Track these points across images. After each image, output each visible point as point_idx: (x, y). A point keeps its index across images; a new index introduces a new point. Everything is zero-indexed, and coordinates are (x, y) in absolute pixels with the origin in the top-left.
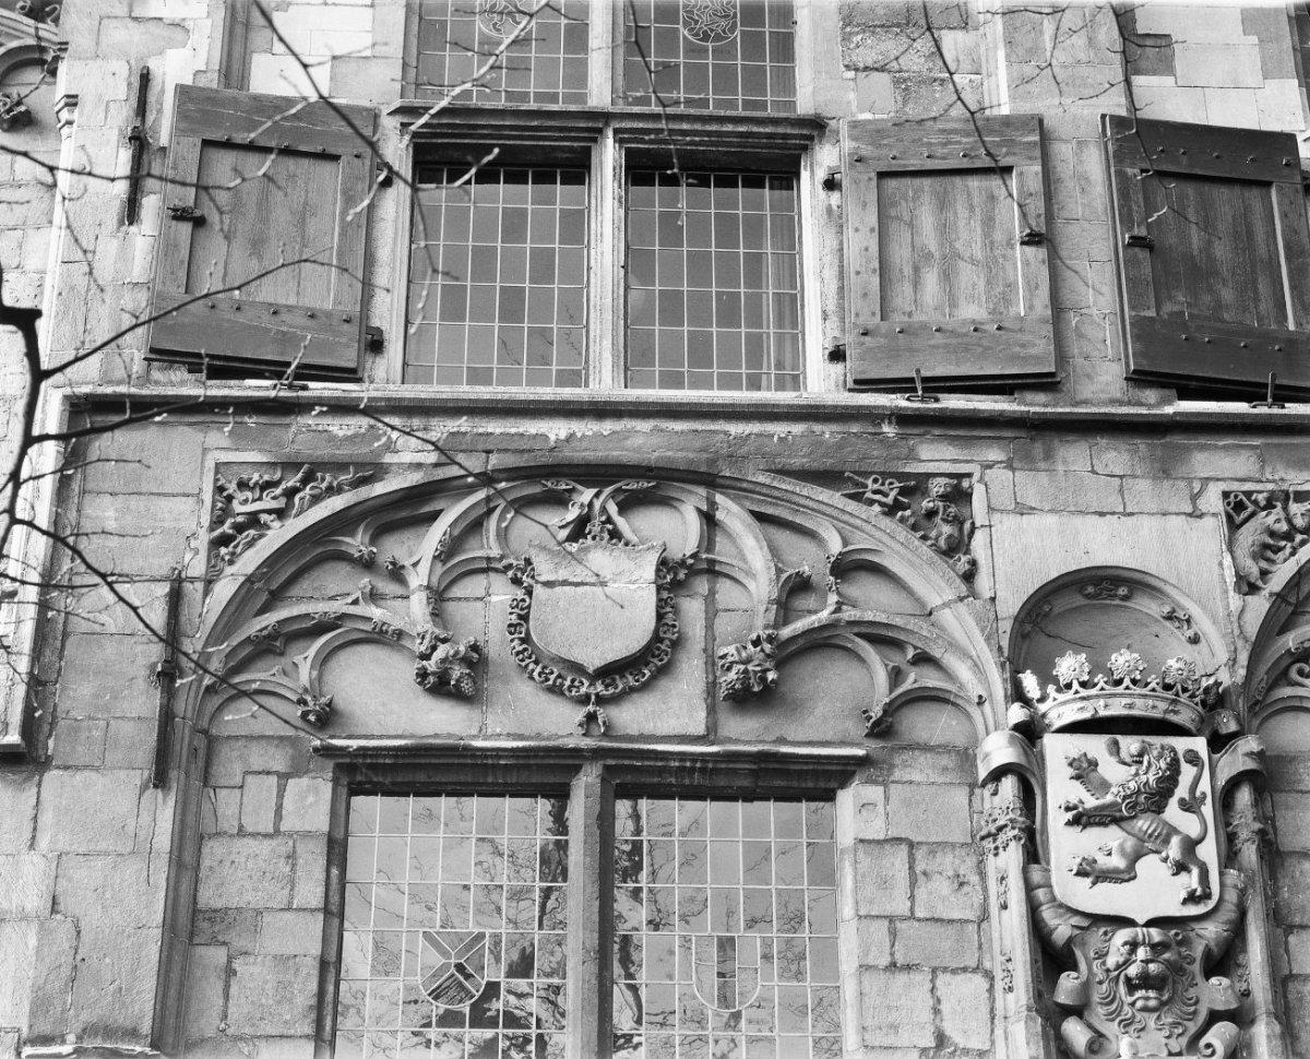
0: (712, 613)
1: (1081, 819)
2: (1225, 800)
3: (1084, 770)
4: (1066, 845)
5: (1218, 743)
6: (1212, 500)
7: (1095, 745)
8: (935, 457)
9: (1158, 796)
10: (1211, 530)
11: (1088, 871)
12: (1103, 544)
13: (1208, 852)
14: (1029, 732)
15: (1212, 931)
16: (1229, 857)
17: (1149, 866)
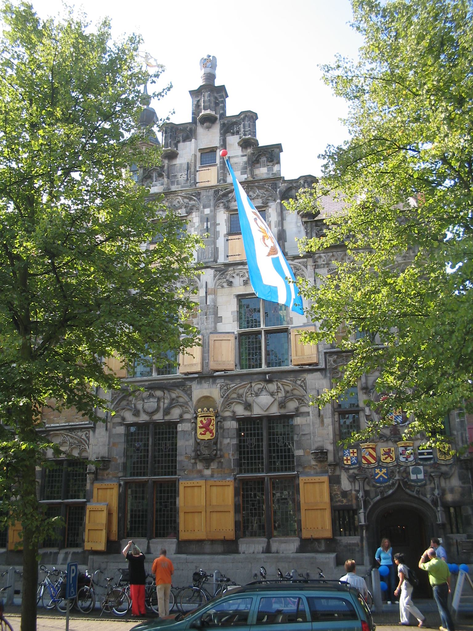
0: (164, 403)
1: (201, 428)
2: (217, 423)
3: (201, 422)
4: (199, 431)
5: (216, 417)
6: (219, 386)
7: (203, 419)
8: (188, 383)
9: (209, 424)
10: (218, 389)
11: (201, 434)
12: (206, 393)
13: (214, 431)
14: (196, 418)
15: (215, 440)
16: (217, 431)
17: (208, 433)
